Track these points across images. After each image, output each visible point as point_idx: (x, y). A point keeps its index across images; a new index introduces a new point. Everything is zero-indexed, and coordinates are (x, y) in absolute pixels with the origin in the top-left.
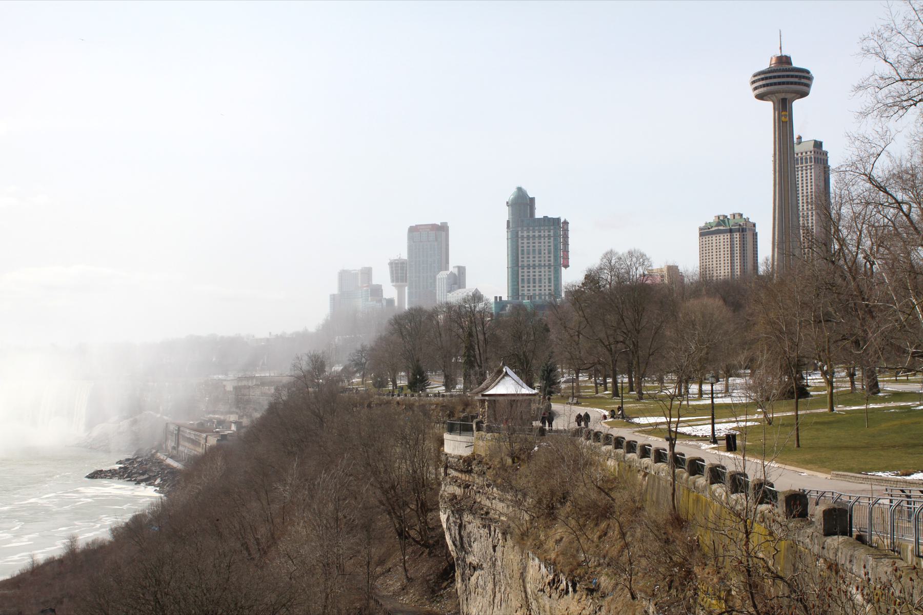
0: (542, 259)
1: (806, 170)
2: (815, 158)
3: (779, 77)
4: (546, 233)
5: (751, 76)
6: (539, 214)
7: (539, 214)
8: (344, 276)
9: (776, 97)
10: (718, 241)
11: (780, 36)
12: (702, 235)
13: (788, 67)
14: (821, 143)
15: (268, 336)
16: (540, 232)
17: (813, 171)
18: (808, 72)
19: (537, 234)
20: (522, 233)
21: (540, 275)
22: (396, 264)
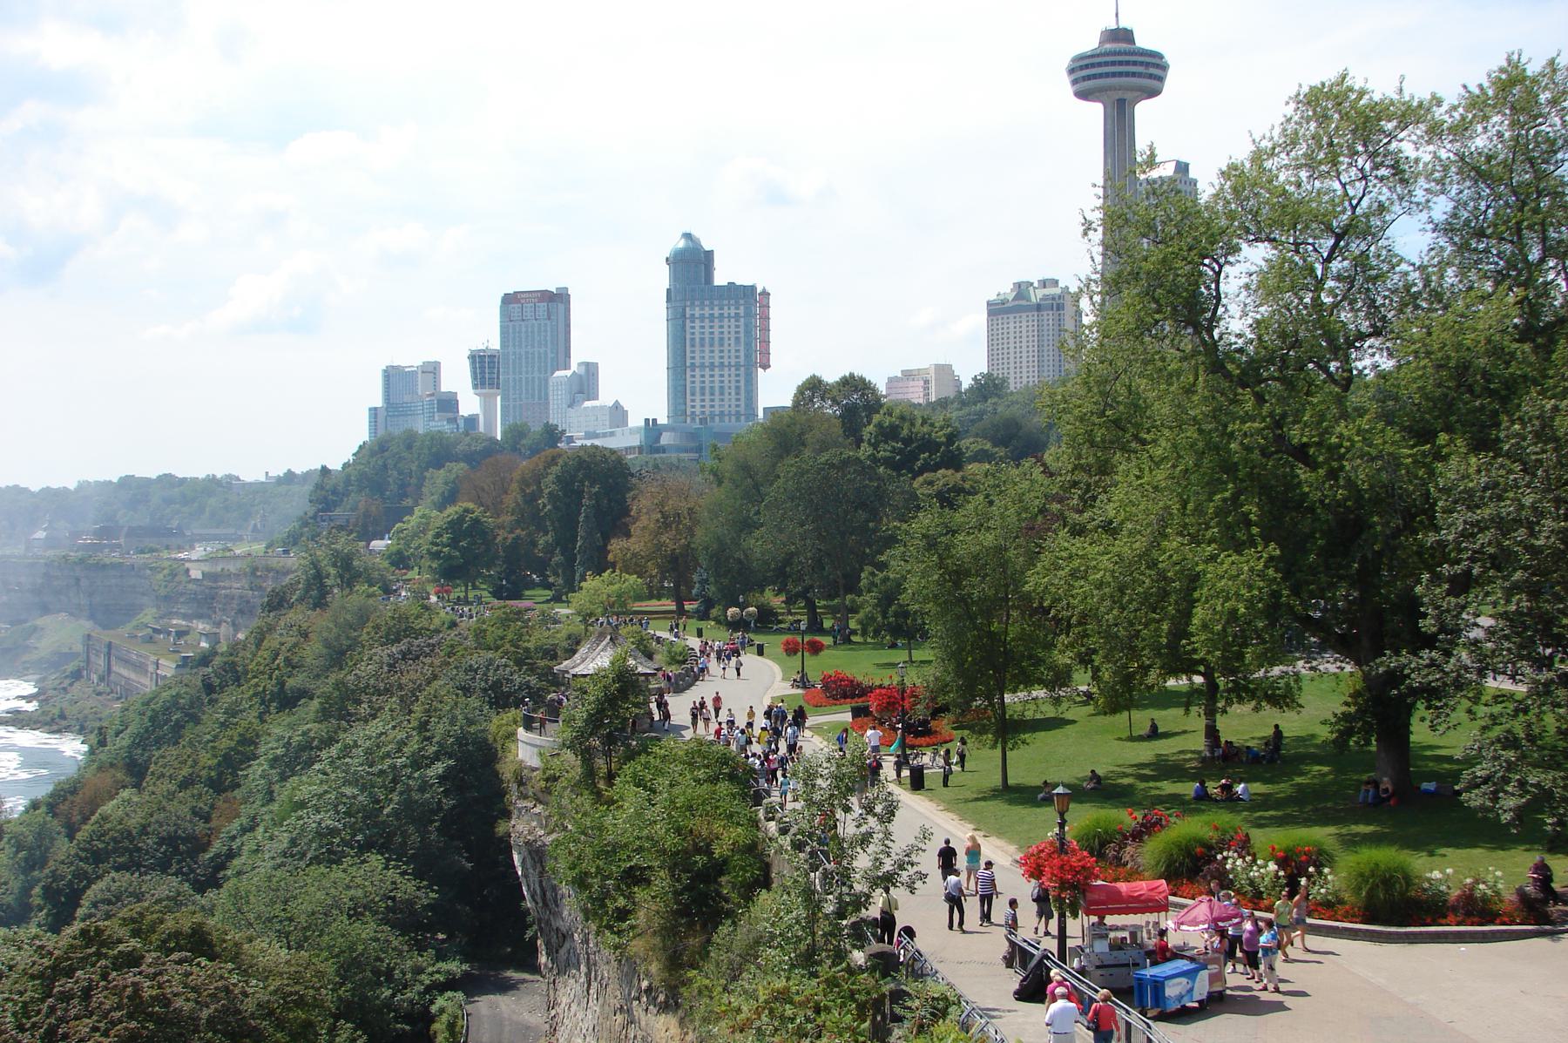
0: (726, 354)
3: (1113, 63)
4: (733, 312)
6: (720, 279)
7: (720, 279)
8: (394, 378)
14: (1187, 165)
16: (721, 309)
18: (1161, 57)
19: (716, 312)
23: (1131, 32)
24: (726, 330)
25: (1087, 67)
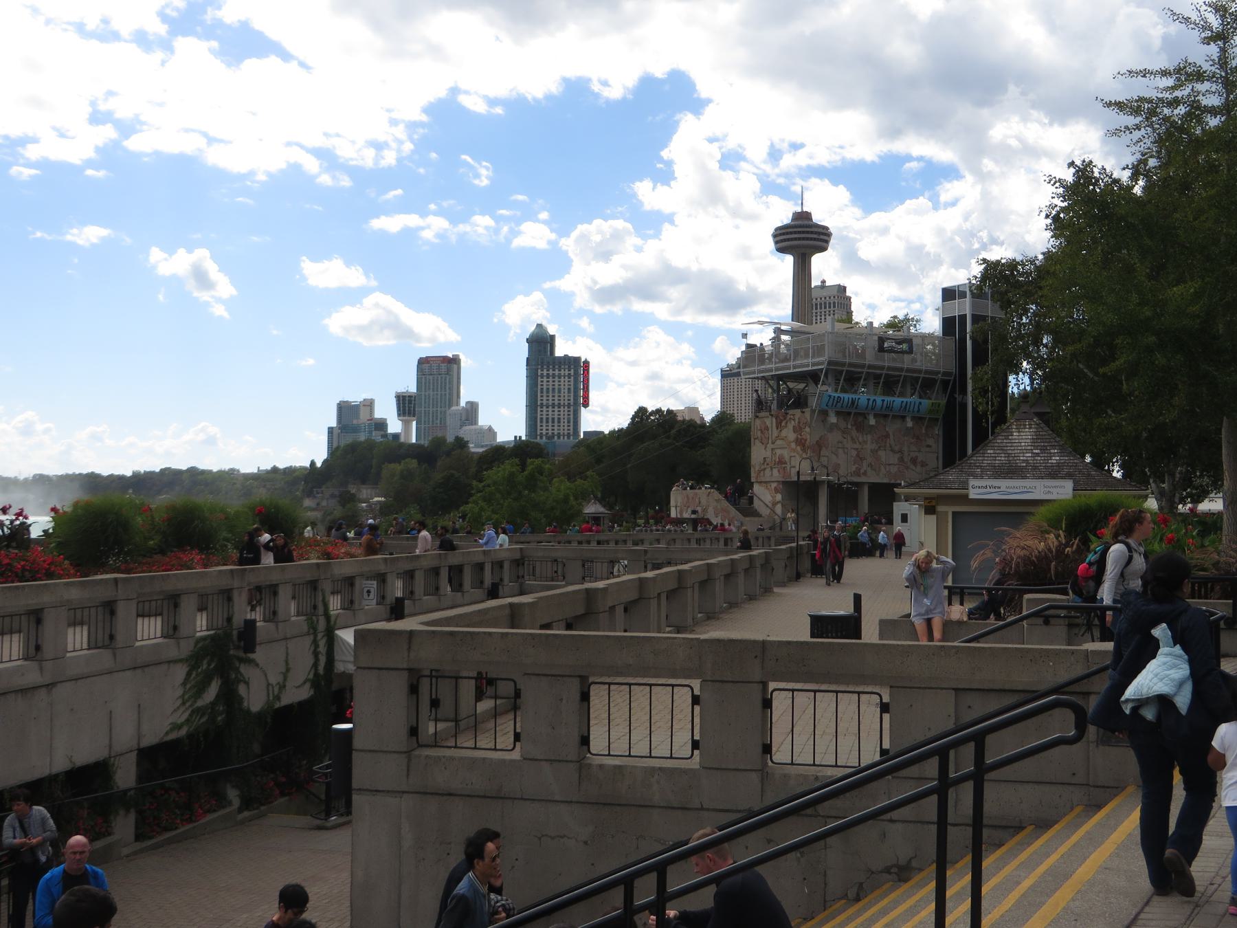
0: (562, 398)
4: (567, 372)
6: (560, 352)
7: (560, 352)
13: (806, 222)
15: (256, 471)
18: (827, 228)
19: (557, 372)
20: (542, 371)
21: (559, 415)
22: (404, 397)
24: (562, 383)
25: (784, 234)
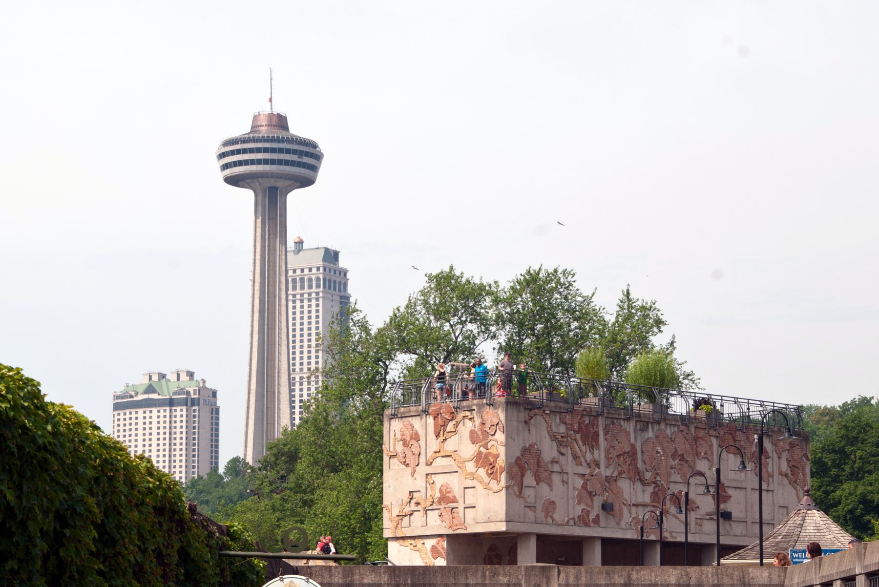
1: (310, 300)
2: (324, 279)
5: (219, 143)
9: (260, 184)
10: (148, 420)
11: (271, 79)
12: (117, 407)
13: (281, 134)
14: (336, 254)
17: (321, 302)
18: (314, 146)
23: (285, 118)
